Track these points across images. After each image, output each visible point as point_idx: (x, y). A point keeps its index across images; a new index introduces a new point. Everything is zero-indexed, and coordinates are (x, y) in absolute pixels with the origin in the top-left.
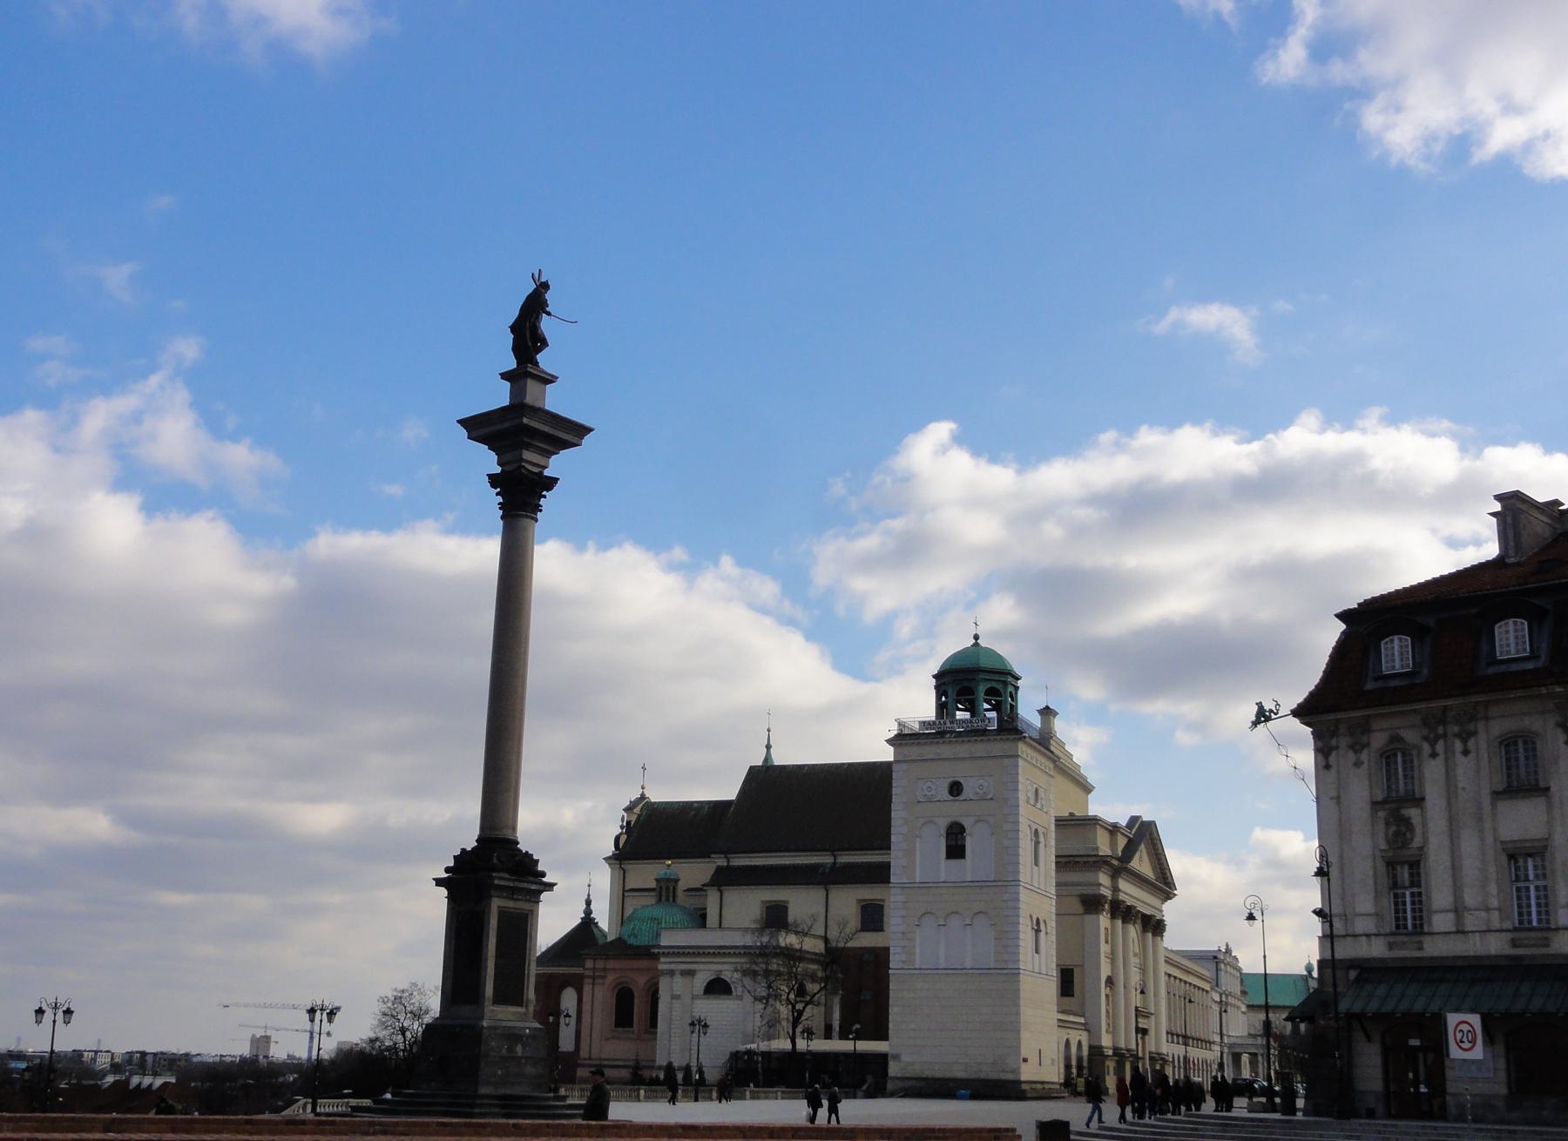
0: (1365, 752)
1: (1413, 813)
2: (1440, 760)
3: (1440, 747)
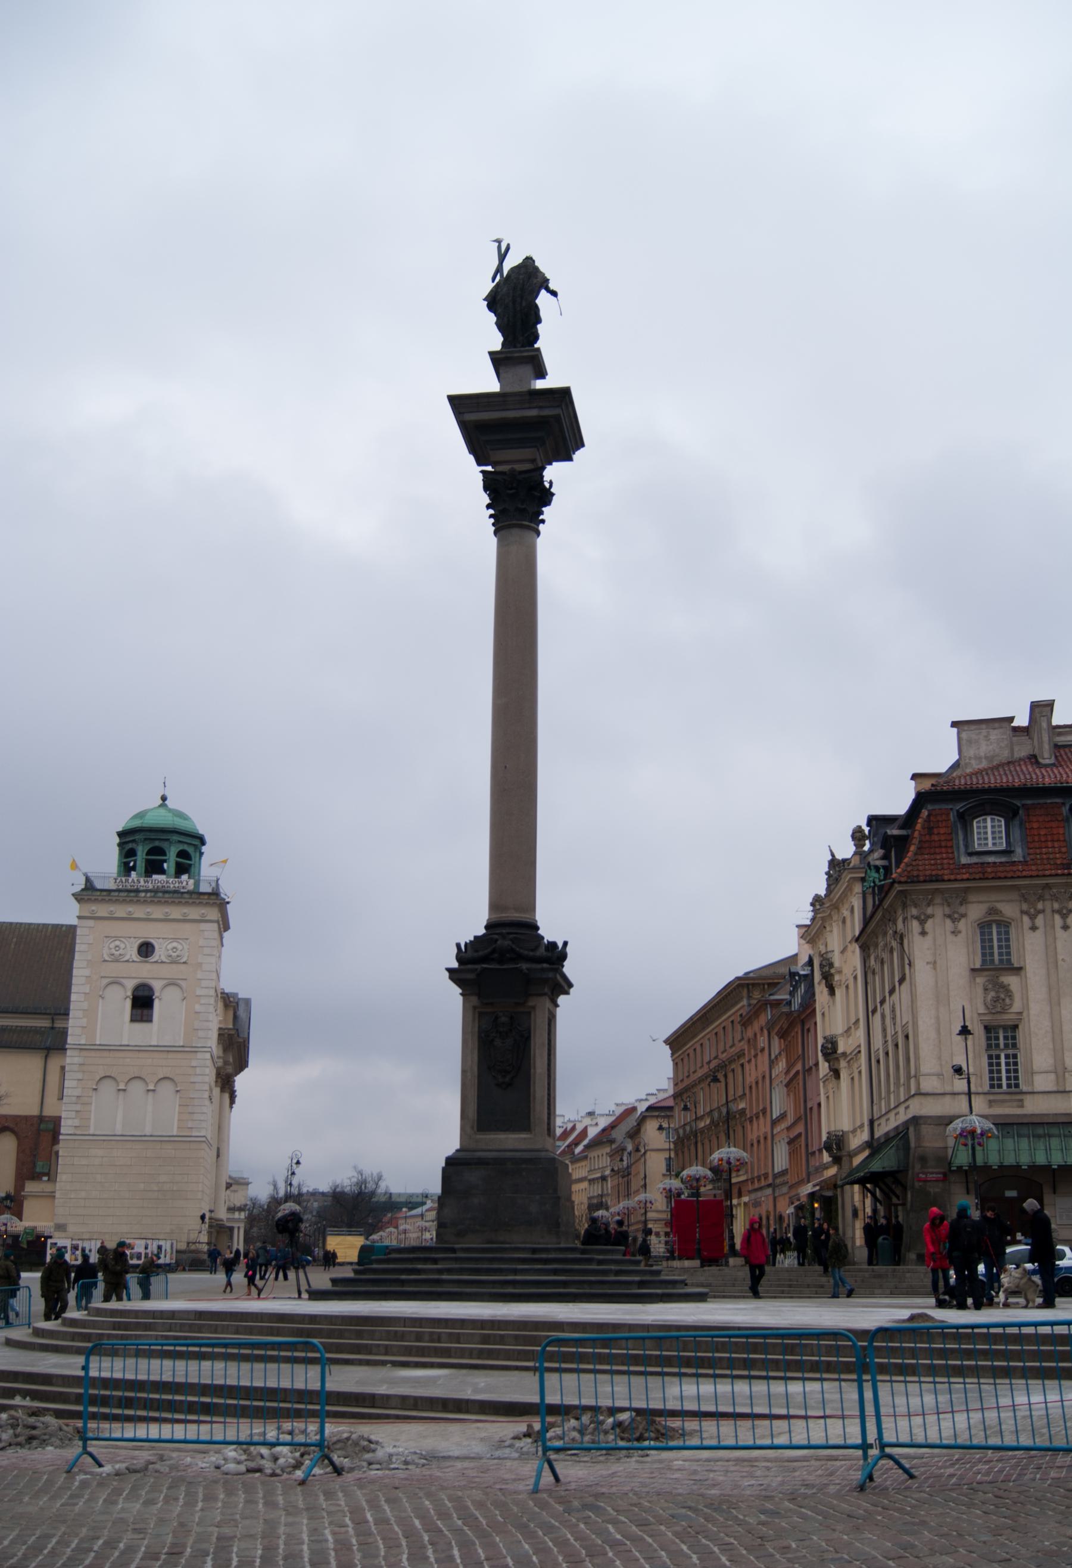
0: (963, 921)
3: (1040, 921)
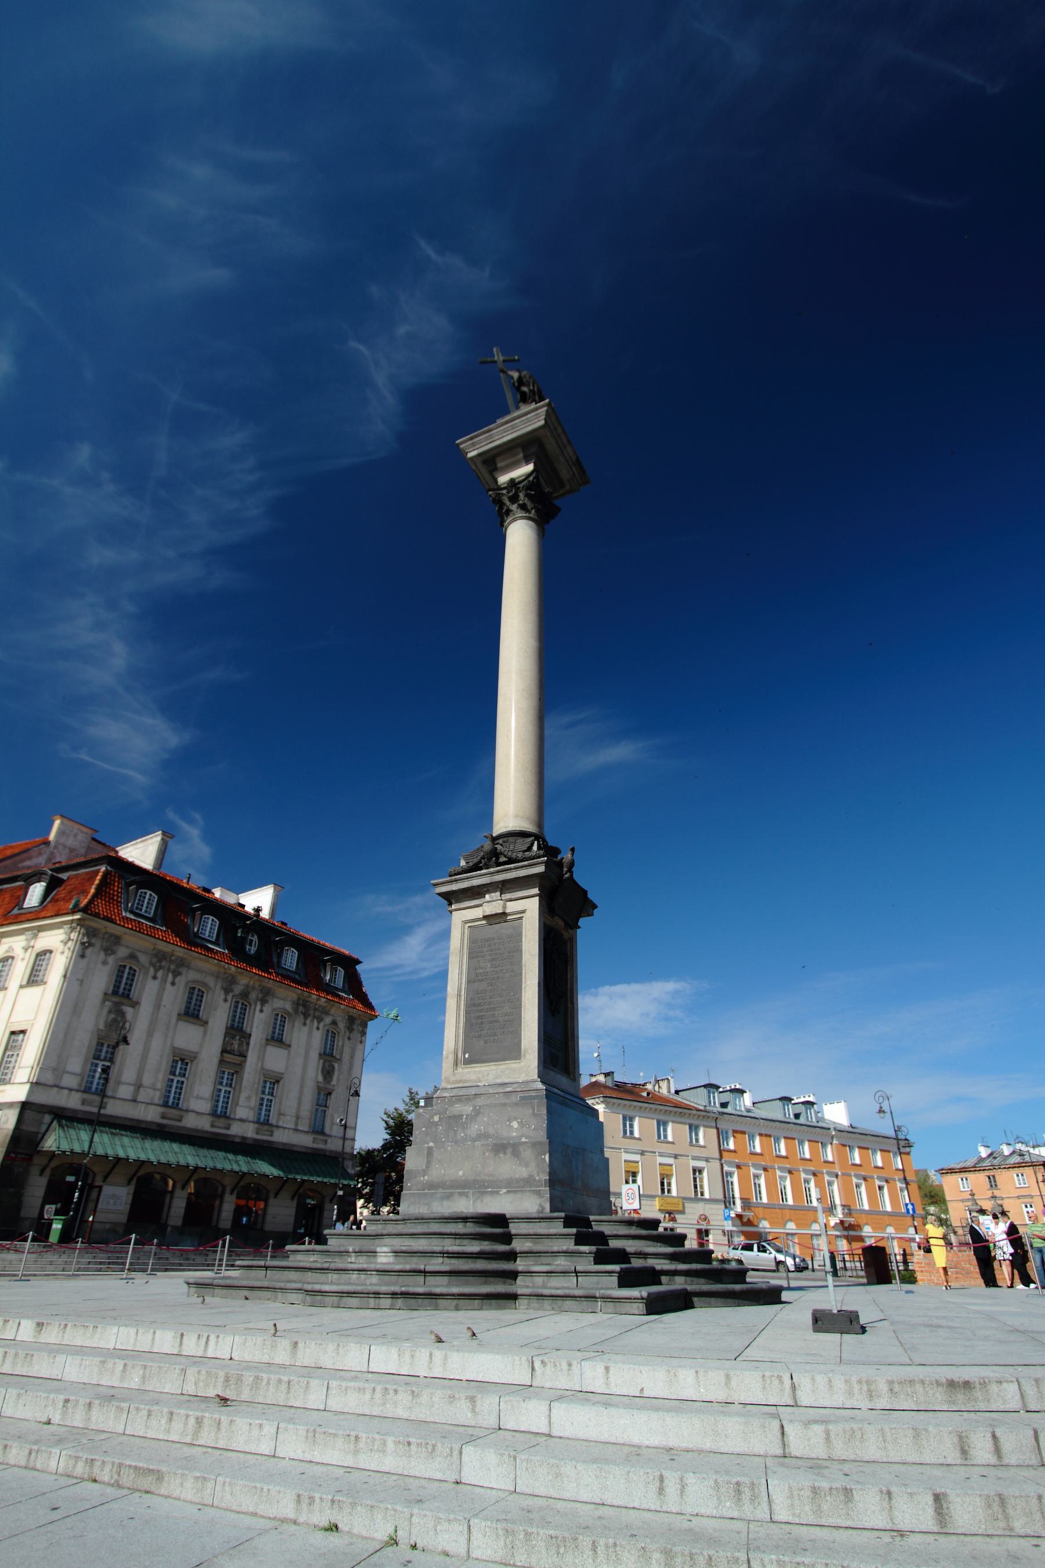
2: (157, 983)
3: (160, 974)
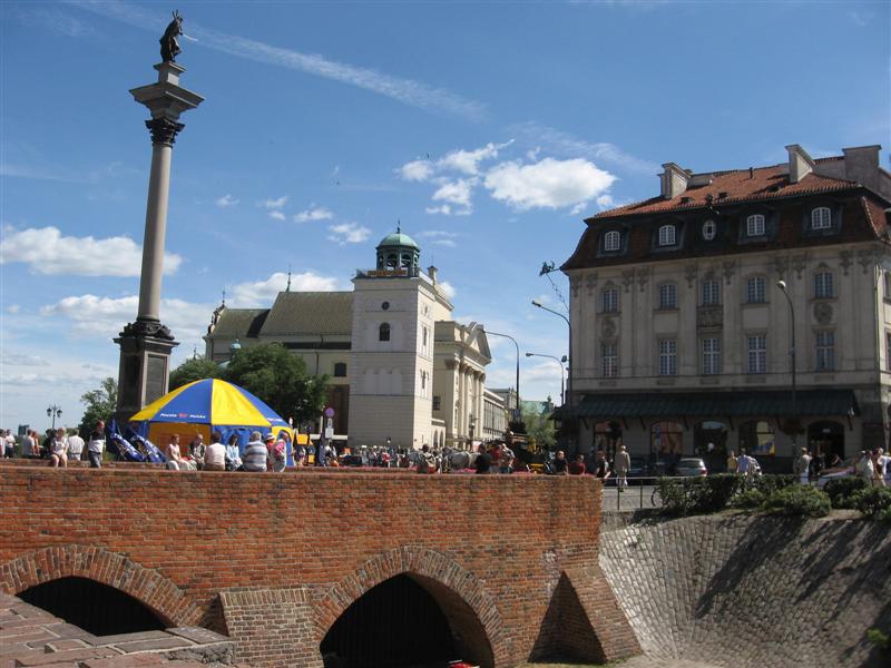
1: (615, 320)
2: (630, 294)
3: (630, 288)
